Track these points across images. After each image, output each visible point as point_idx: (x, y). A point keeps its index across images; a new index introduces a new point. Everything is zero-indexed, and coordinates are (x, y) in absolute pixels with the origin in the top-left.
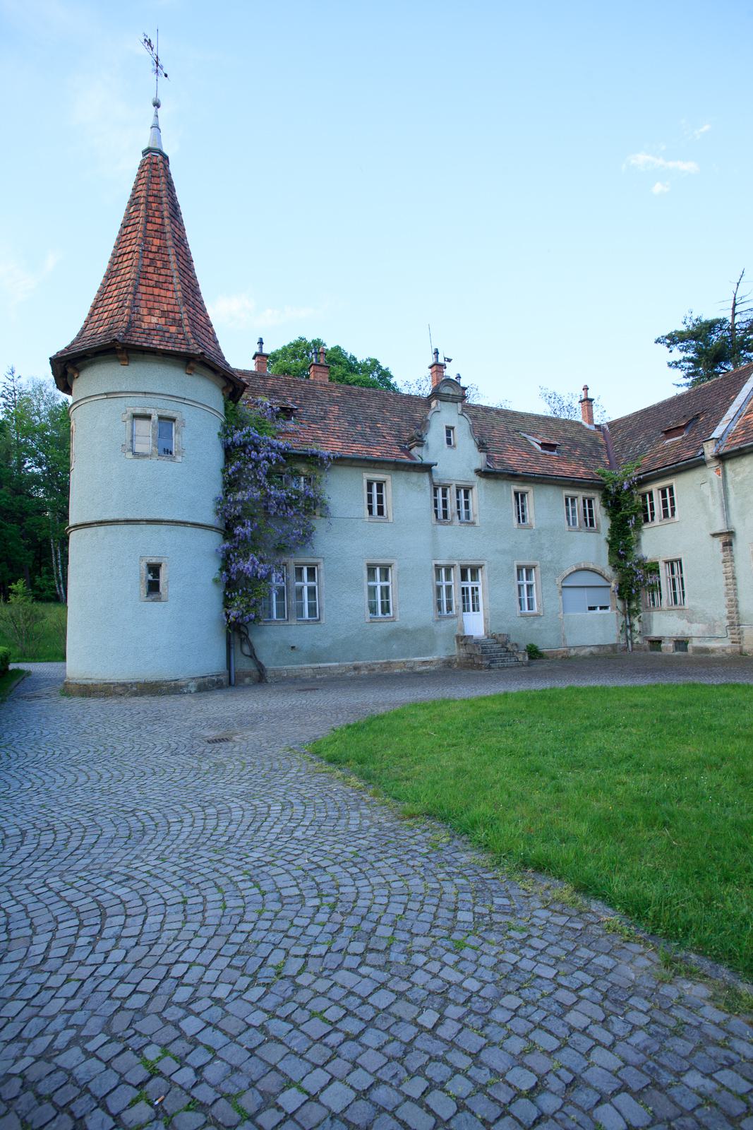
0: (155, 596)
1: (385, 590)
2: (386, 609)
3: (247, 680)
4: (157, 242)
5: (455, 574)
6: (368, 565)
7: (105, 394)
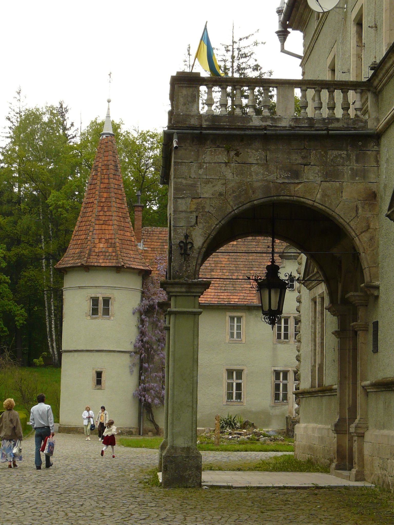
0: (99, 386)
1: (239, 386)
2: (239, 396)
3: (150, 433)
4: (105, 195)
5: (291, 376)
6: (227, 370)
7: (78, 287)
